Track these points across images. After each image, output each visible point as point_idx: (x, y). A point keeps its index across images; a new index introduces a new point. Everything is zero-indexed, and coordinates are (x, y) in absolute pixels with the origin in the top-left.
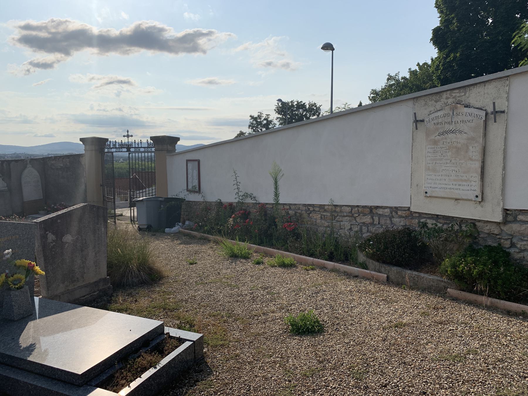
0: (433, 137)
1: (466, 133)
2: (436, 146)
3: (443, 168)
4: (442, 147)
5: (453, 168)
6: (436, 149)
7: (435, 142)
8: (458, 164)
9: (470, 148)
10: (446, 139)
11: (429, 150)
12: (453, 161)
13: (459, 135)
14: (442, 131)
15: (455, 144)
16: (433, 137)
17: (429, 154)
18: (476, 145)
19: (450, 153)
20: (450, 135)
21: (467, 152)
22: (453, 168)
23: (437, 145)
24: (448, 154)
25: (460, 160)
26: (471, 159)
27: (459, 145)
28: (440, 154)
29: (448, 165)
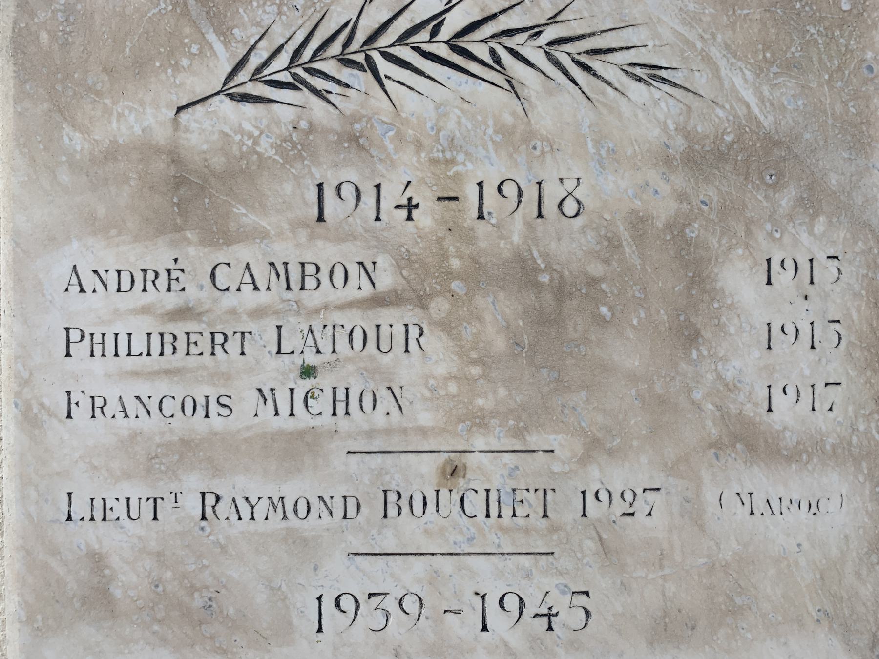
0: (140, 116)
1: (652, 74)
2: (197, 257)
3: (356, 579)
4: (308, 274)
5: (488, 575)
6: (197, 292)
7: (189, 195)
8: (566, 512)
9: (738, 280)
10: (354, 140)
11: (94, 310)
12: (488, 470)
13: (553, 104)
14: (288, 29)
15: (509, 231)
16: (140, 116)
17: (95, 375)
18: (808, 241)
19: (438, 356)
20: (431, 99)
21: (690, 337)
22: (488, 575)
23: (220, 234)
24: (408, 370)
25: (595, 447)
26: (749, 440)
27: (568, 246)
28: (277, 372)
29: (409, 530)
